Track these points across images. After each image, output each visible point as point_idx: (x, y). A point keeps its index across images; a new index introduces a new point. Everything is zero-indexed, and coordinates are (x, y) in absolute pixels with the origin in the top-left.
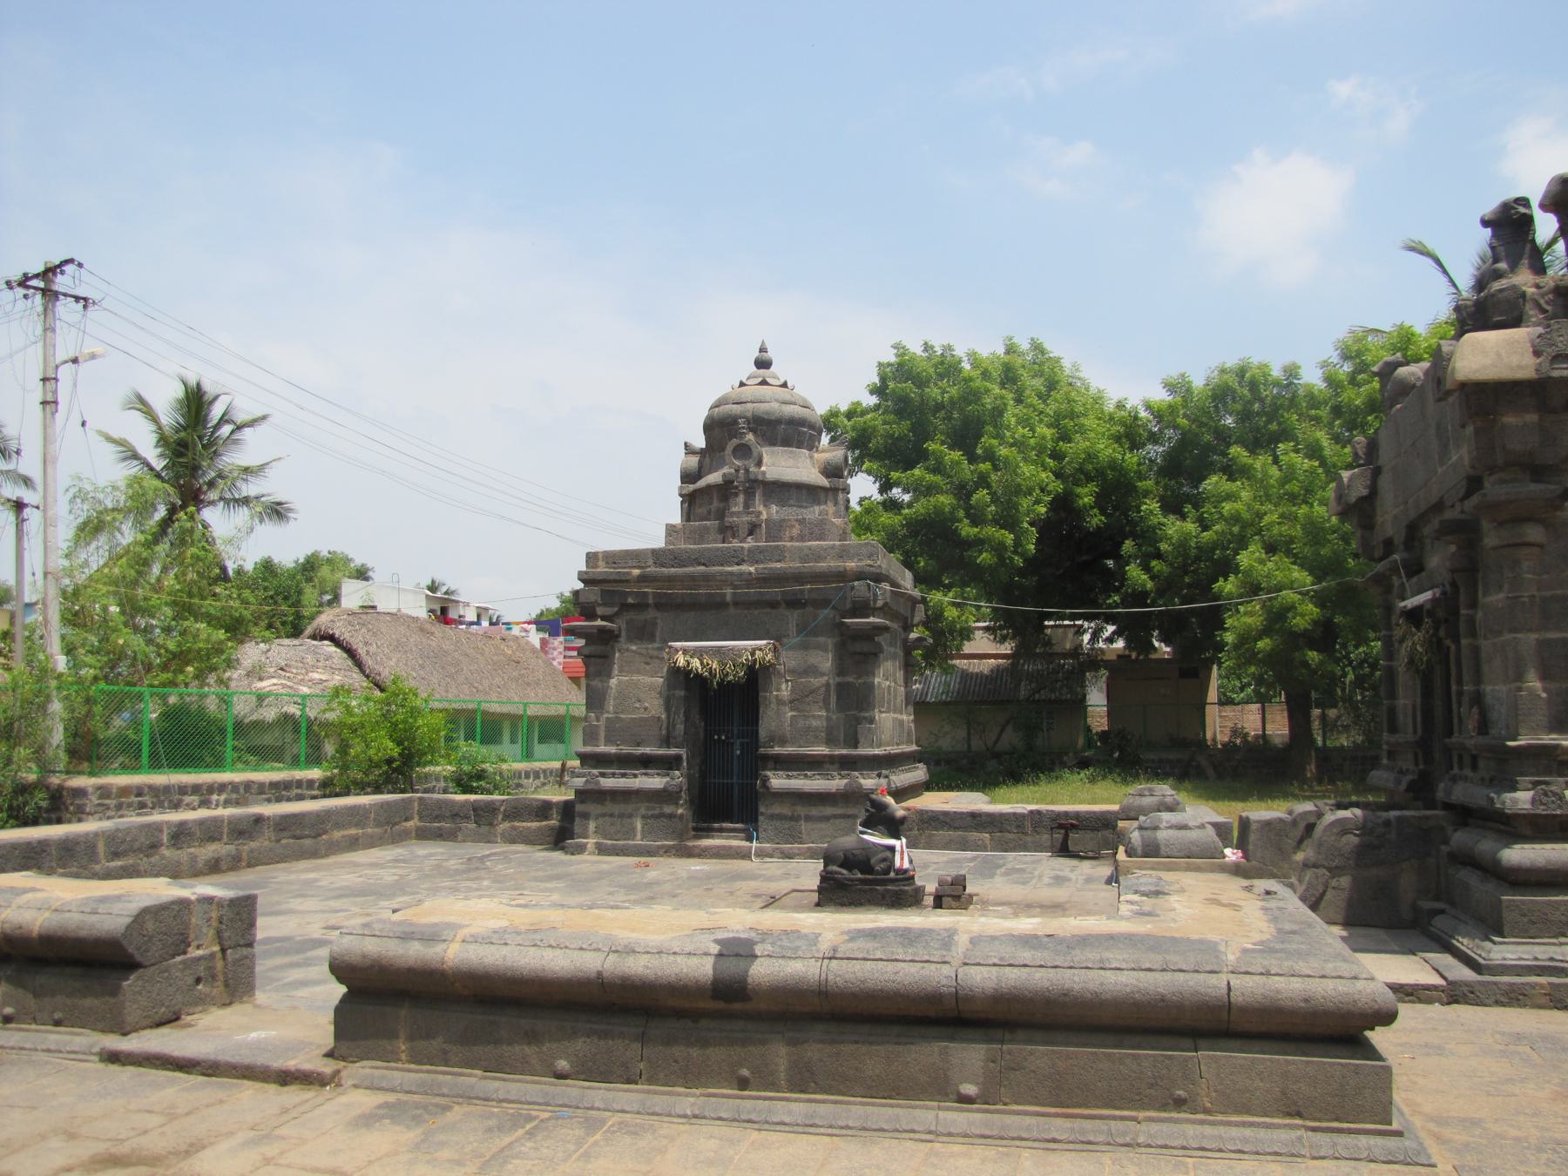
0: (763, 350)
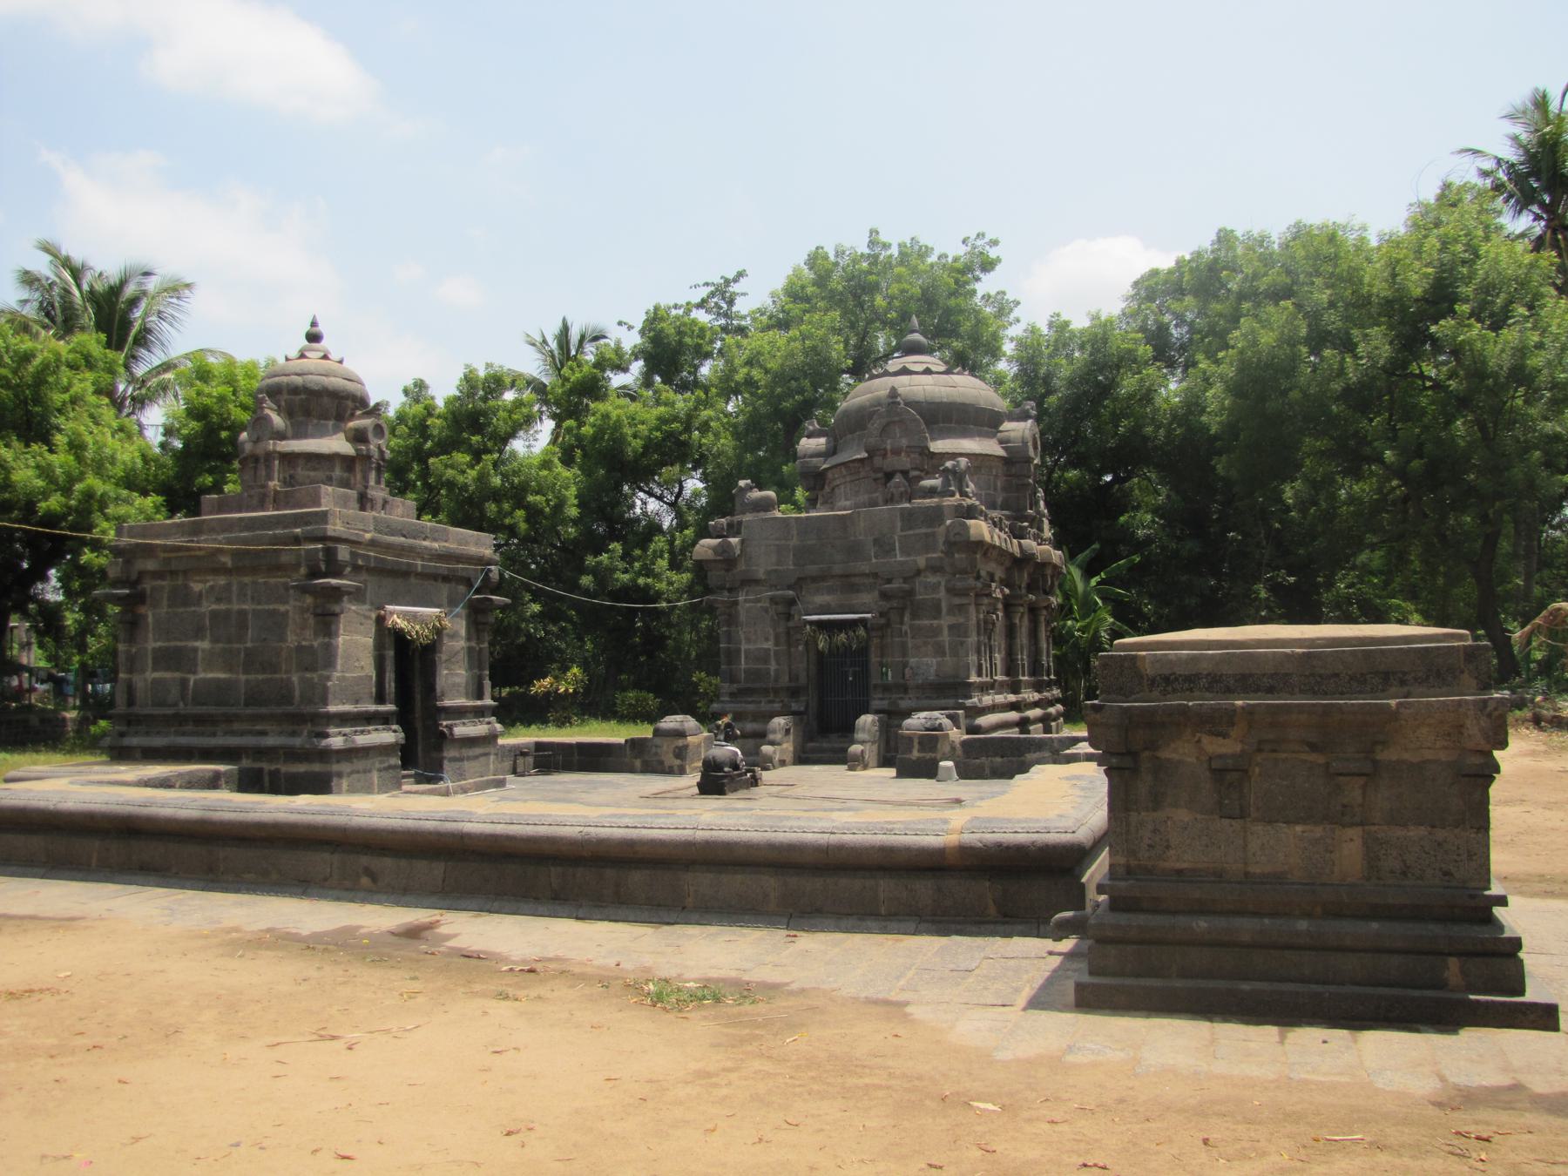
0: (314, 324)
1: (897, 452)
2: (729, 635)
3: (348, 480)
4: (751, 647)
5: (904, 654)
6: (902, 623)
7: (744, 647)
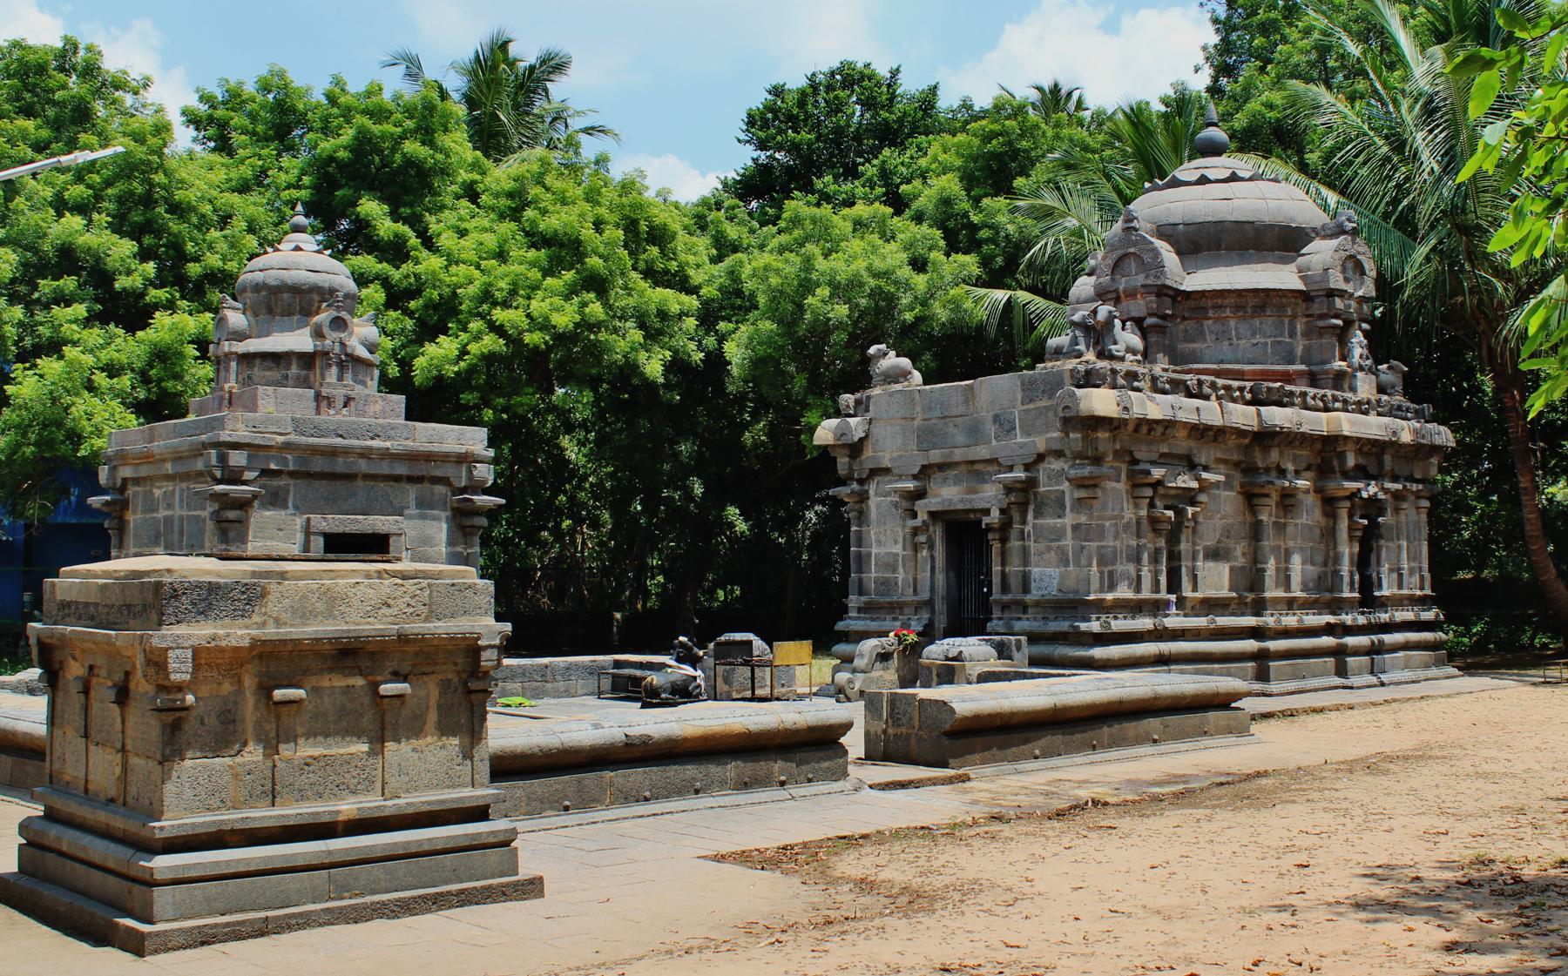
1: (1131, 294)
2: (859, 534)
3: (306, 378)
4: (882, 551)
5: (1025, 561)
6: (1024, 522)
7: (874, 551)
